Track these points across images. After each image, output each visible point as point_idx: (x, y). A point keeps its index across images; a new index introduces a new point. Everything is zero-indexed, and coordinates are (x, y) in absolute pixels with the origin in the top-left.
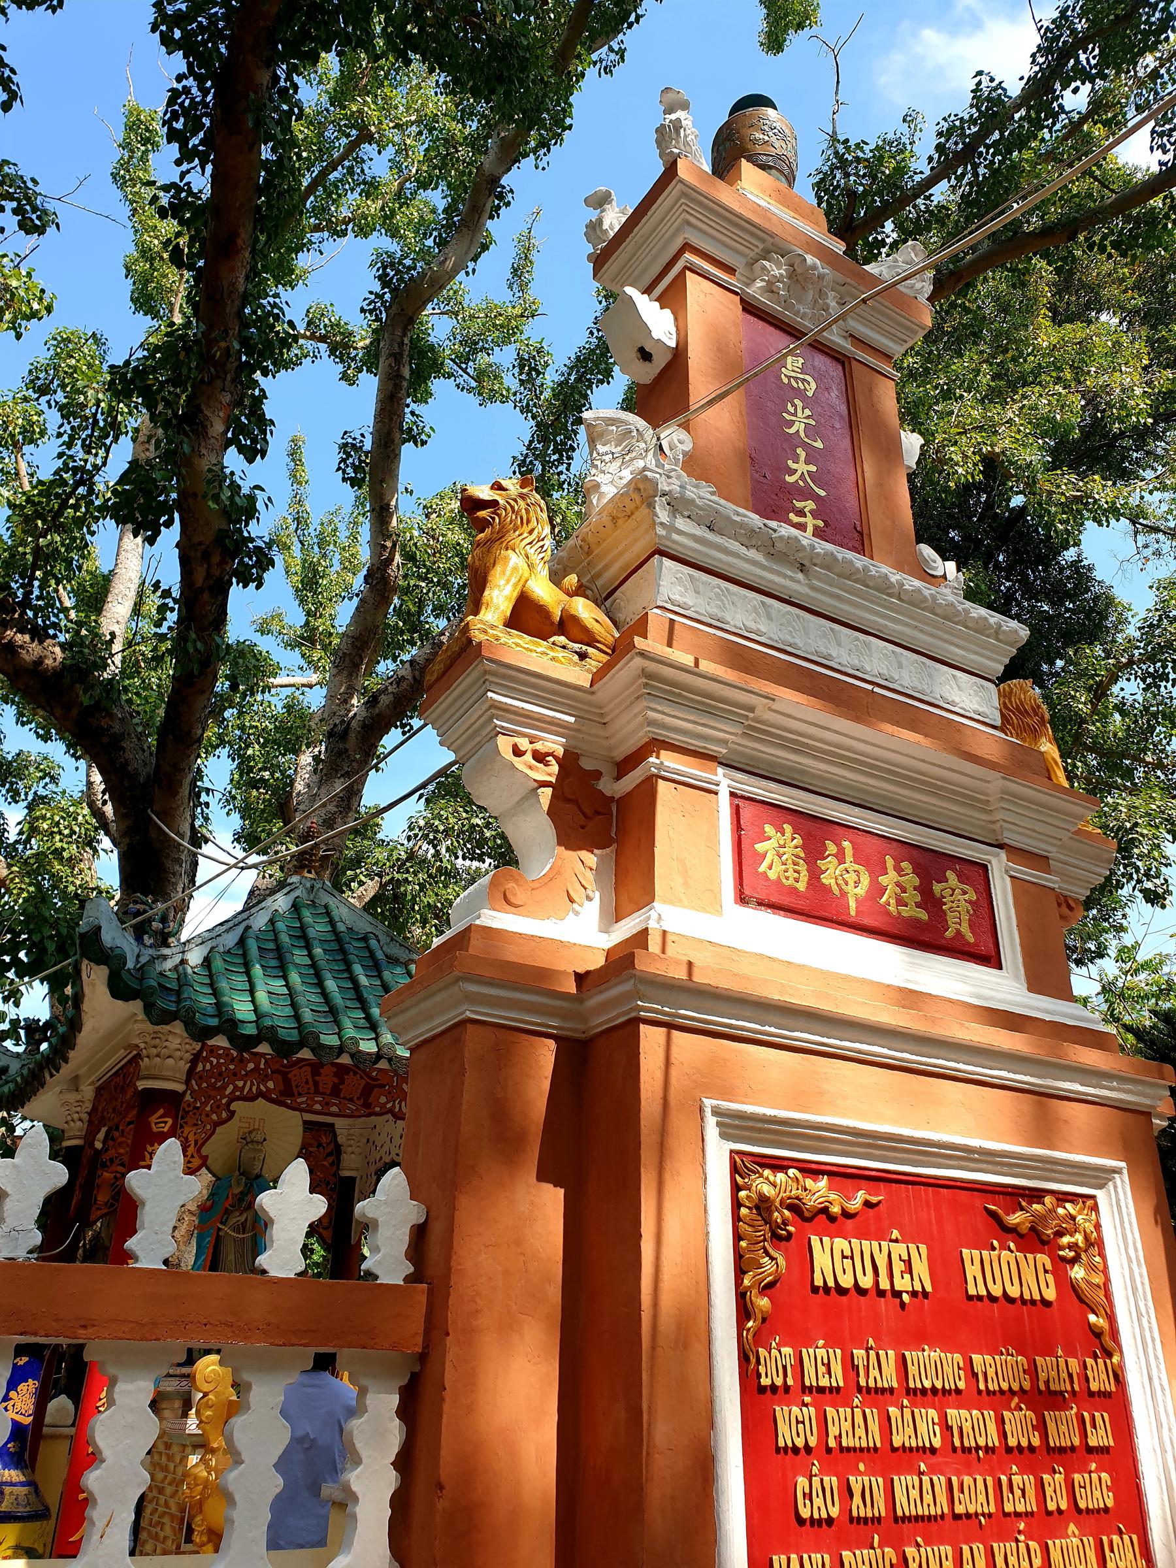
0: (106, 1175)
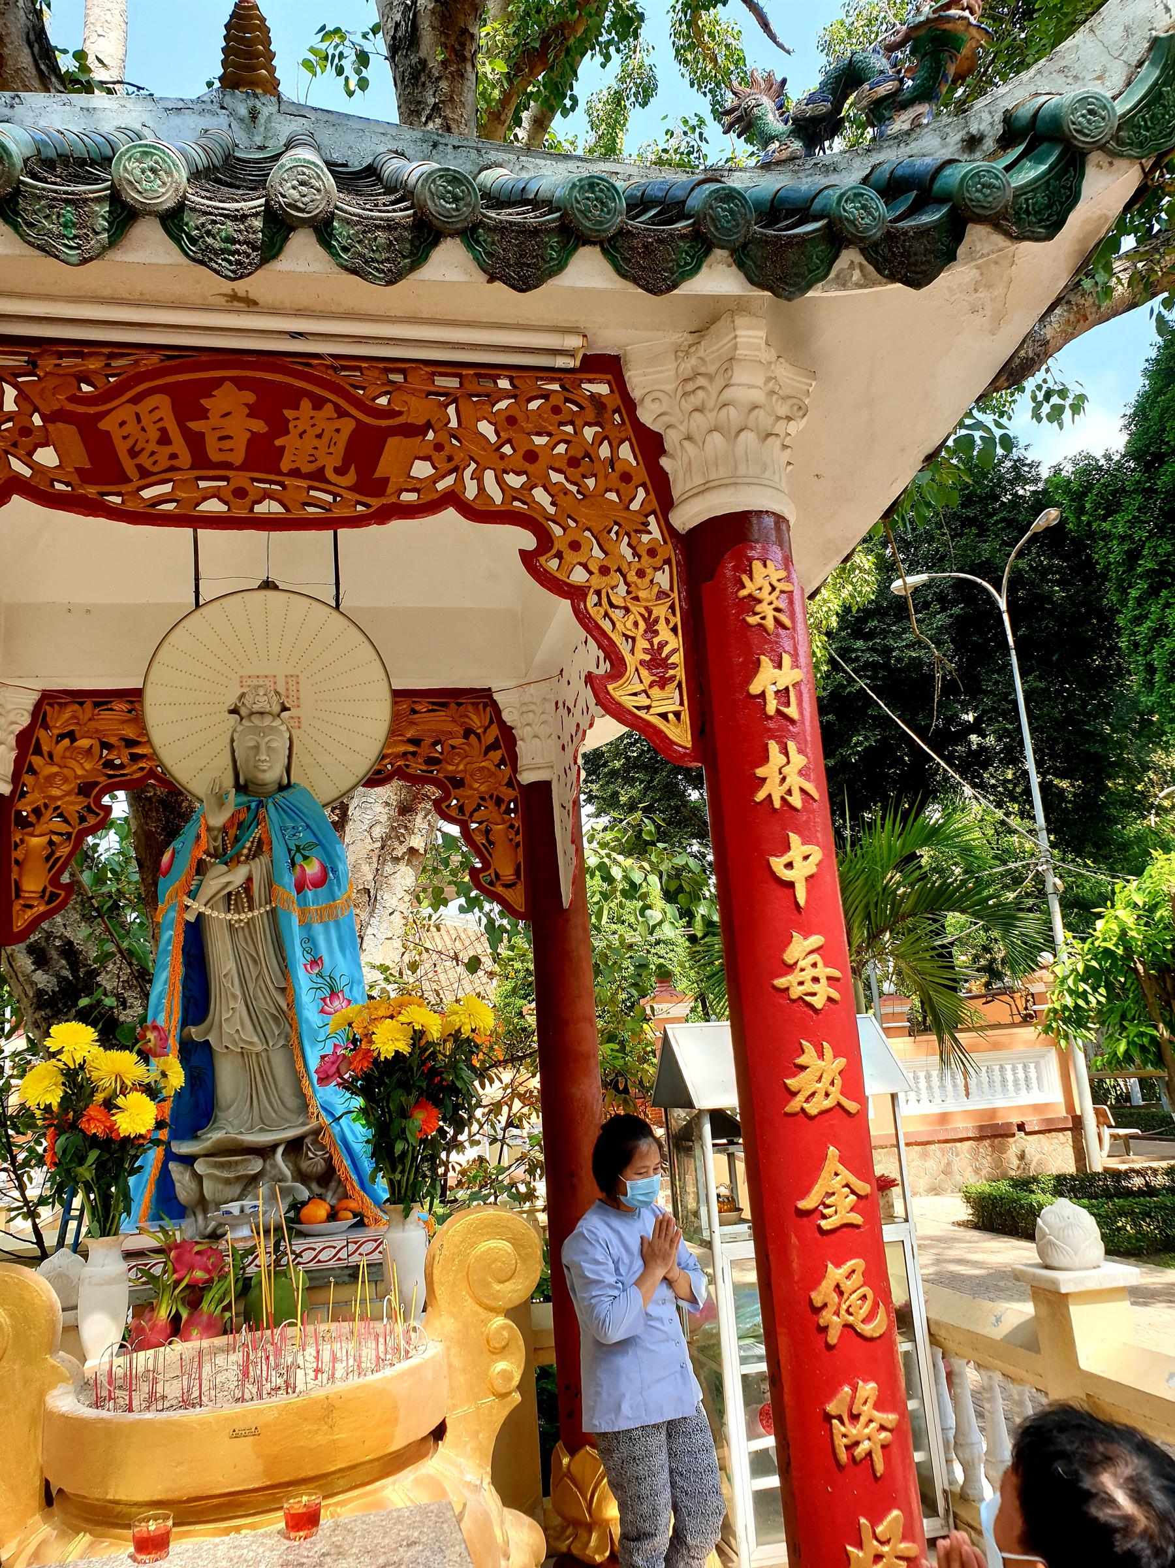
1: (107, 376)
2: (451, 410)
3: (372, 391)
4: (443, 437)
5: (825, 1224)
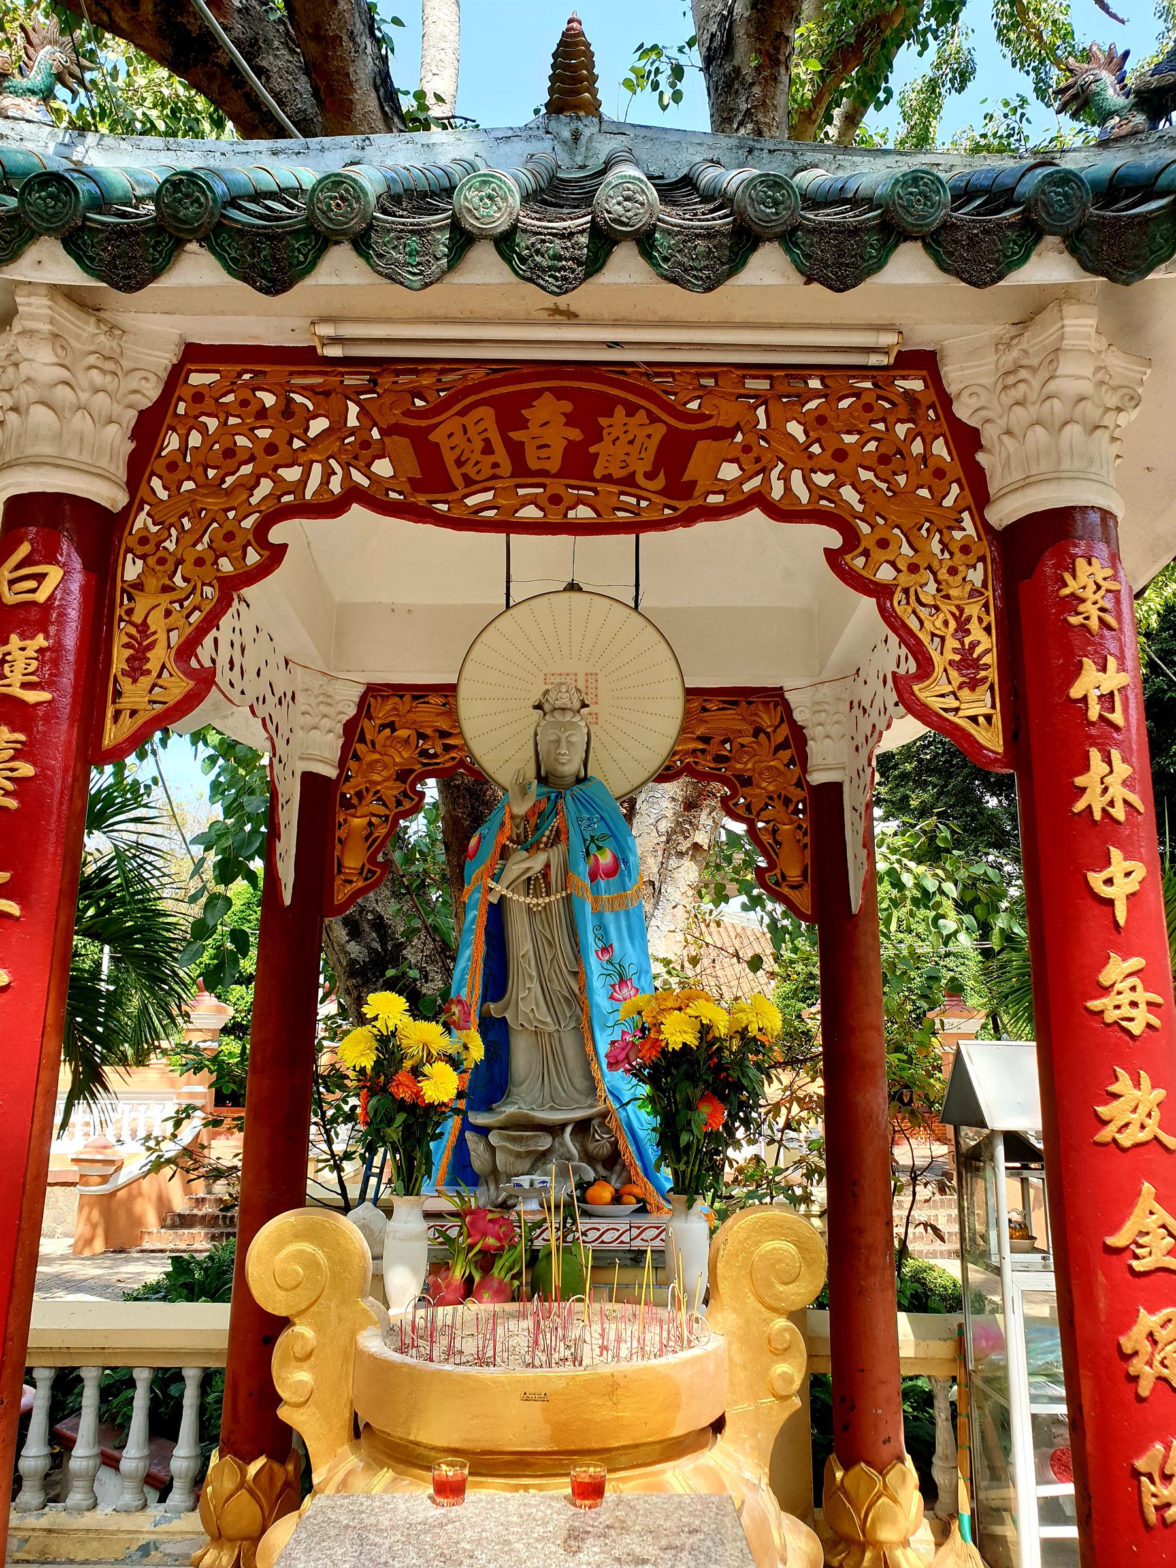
0: (356, 821)
1: (438, 391)
2: (761, 412)
3: (683, 396)
4: (752, 439)
5: (1137, 1265)
